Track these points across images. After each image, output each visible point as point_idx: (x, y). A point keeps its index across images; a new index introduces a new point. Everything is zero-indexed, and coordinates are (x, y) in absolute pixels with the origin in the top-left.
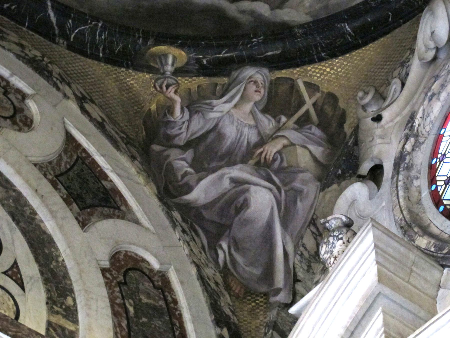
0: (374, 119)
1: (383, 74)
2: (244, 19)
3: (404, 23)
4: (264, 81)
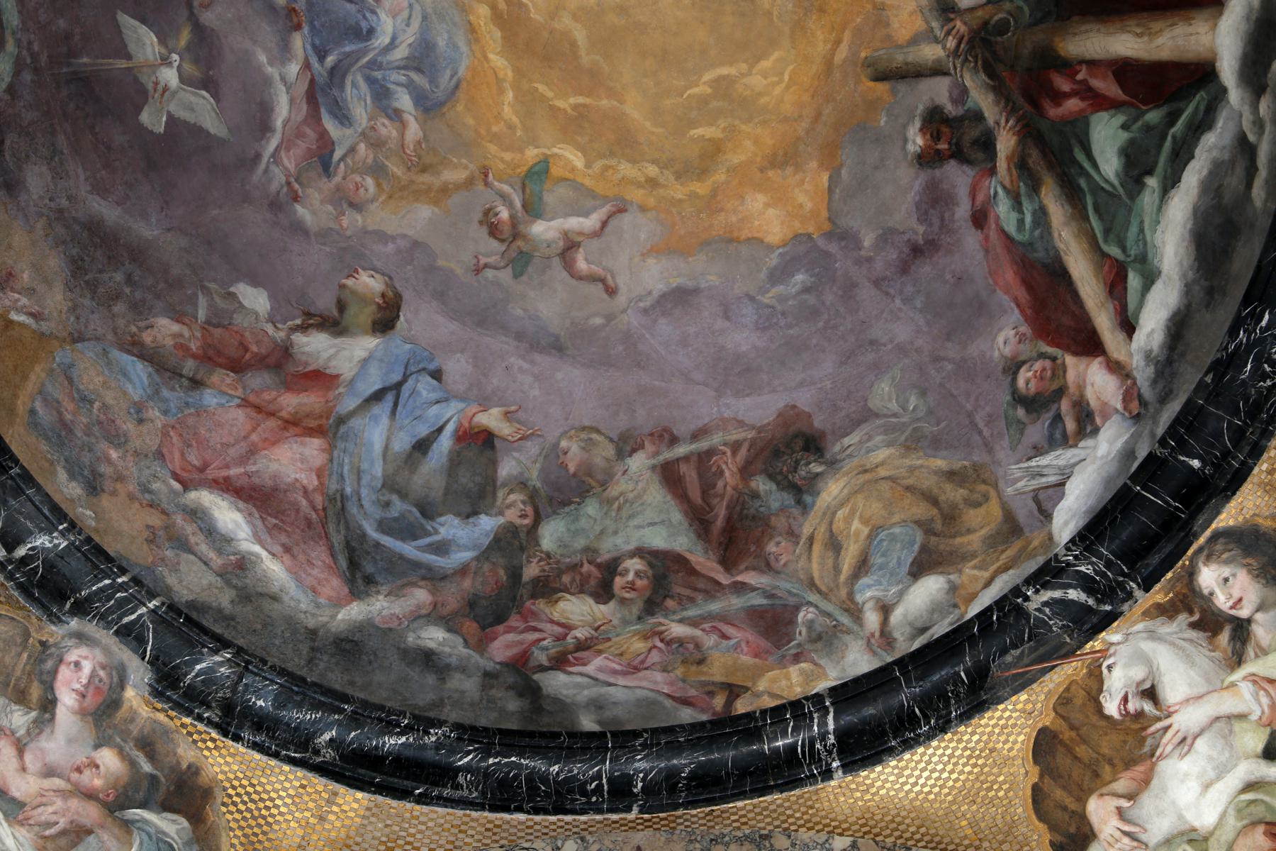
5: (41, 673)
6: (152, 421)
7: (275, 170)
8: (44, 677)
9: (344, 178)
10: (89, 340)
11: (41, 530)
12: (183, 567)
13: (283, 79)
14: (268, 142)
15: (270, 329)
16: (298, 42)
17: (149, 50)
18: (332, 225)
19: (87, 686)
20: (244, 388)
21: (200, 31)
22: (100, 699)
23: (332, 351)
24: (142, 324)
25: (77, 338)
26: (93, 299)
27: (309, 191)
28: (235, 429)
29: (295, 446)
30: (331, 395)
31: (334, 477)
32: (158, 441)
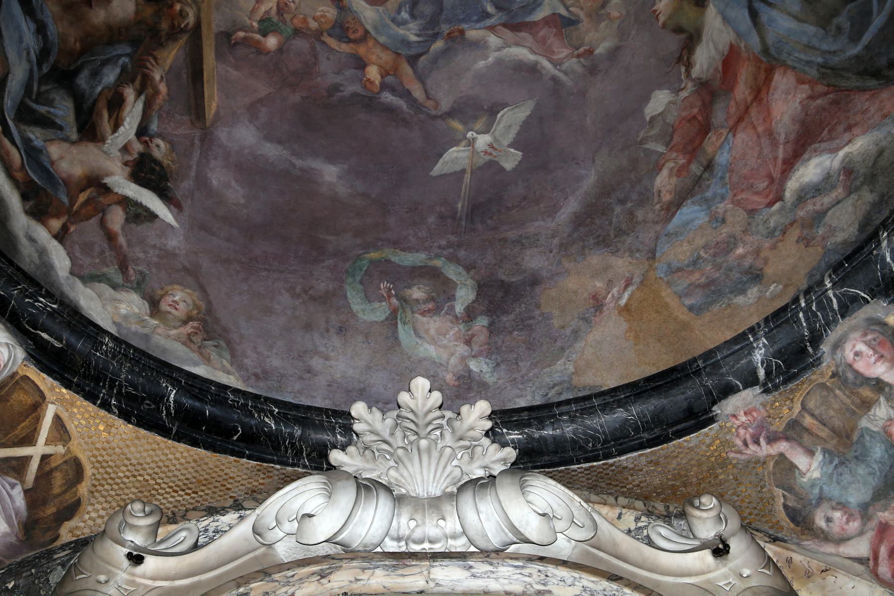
0: (130, 556)
1: (171, 499)
2: (26, 250)
3: (250, 458)
4: (5, 366)
5: (854, 384)
6: (726, 211)
7: (564, 67)
8: (858, 382)
9: (582, 9)
10: (656, 246)
11: (750, 354)
12: (834, 223)
13: (499, 49)
14: (543, 68)
15: (684, 94)
16: (473, 34)
17: (462, 154)
18: (615, 26)
19: (875, 352)
20: (722, 127)
21: (451, 114)
22: (888, 344)
23: (711, 45)
24: (656, 199)
25: (652, 255)
26: (628, 234)
27: (587, 40)
28: (750, 143)
29: (776, 96)
30: (744, 55)
31: (807, 69)
32: (741, 211)
